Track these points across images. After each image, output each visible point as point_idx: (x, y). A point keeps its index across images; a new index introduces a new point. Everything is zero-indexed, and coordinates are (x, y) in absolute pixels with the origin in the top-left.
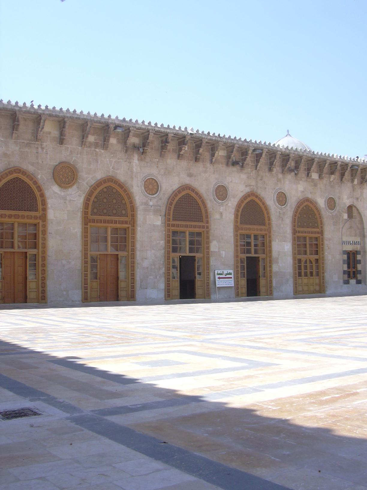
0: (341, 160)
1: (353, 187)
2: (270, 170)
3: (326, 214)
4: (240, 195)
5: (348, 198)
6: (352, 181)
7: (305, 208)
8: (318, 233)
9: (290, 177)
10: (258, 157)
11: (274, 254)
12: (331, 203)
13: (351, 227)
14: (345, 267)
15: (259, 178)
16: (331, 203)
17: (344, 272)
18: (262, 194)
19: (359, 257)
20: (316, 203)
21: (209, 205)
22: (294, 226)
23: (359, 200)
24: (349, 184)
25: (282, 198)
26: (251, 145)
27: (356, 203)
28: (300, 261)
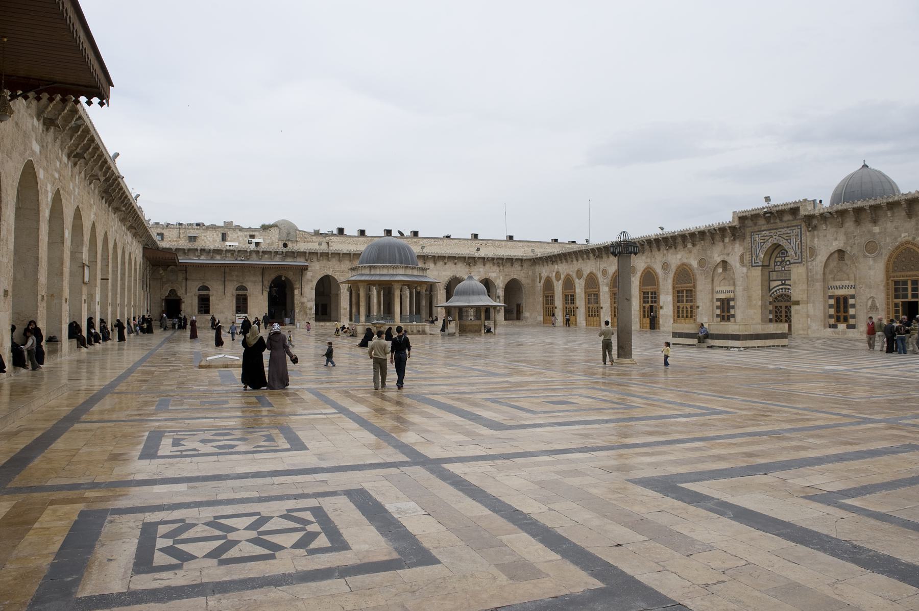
2: (659, 250)
4: (642, 269)
10: (642, 245)
11: (661, 304)
12: (702, 263)
14: (718, 312)
17: (718, 316)
19: (732, 303)
24: (721, 244)
27: (726, 259)
28: (678, 307)
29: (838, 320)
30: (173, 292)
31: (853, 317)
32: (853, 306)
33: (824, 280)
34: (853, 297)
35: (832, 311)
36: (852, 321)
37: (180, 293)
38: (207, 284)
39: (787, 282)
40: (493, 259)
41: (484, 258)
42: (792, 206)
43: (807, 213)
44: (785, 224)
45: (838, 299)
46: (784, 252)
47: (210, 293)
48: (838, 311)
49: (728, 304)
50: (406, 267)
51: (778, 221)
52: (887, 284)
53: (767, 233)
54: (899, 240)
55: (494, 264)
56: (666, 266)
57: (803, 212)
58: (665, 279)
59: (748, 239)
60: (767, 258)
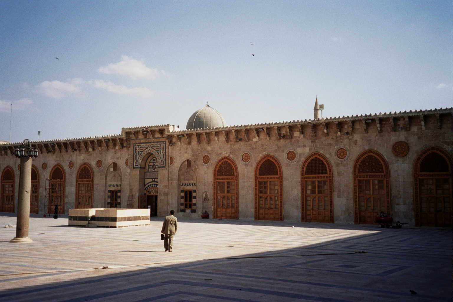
0: (96, 139)
1: (115, 151)
2: (67, 151)
3: (96, 170)
5: (111, 158)
6: (115, 148)
7: (87, 168)
8: (90, 181)
9: (77, 152)
10: (53, 146)
11: (67, 193)
12: (99, 163)
13: (114, 176)
15: (61, 156)
16: (99, 163)
18: (63, 164)
19: (119, 194)
20: (90, 165)
21: (40, 171)
22: (77, 178)
23: (119, 159)
24: (113, 151)
25: (71, 165)
26: (48, 143)
29: (186, 207)
31: (195, 204)
32: (195, 197)
33: (179, 179)
34: (195, 191)
35: (182, 201)
36: (194, 207)
39: (156, 180)
42: (160, 128)
43: (169, 134)
44: (155, 140)
45: (186, 192)
46: (154, 159)
48: (186, 201)
49: (116, 194)
51: (151, 137)
52: (214, 183)
53: (144, 145)
54: (221, 156)
56: (71, 165)
57: (166, 133)
58: (71, 175)
59: (132, 147)
60: (143, 163)
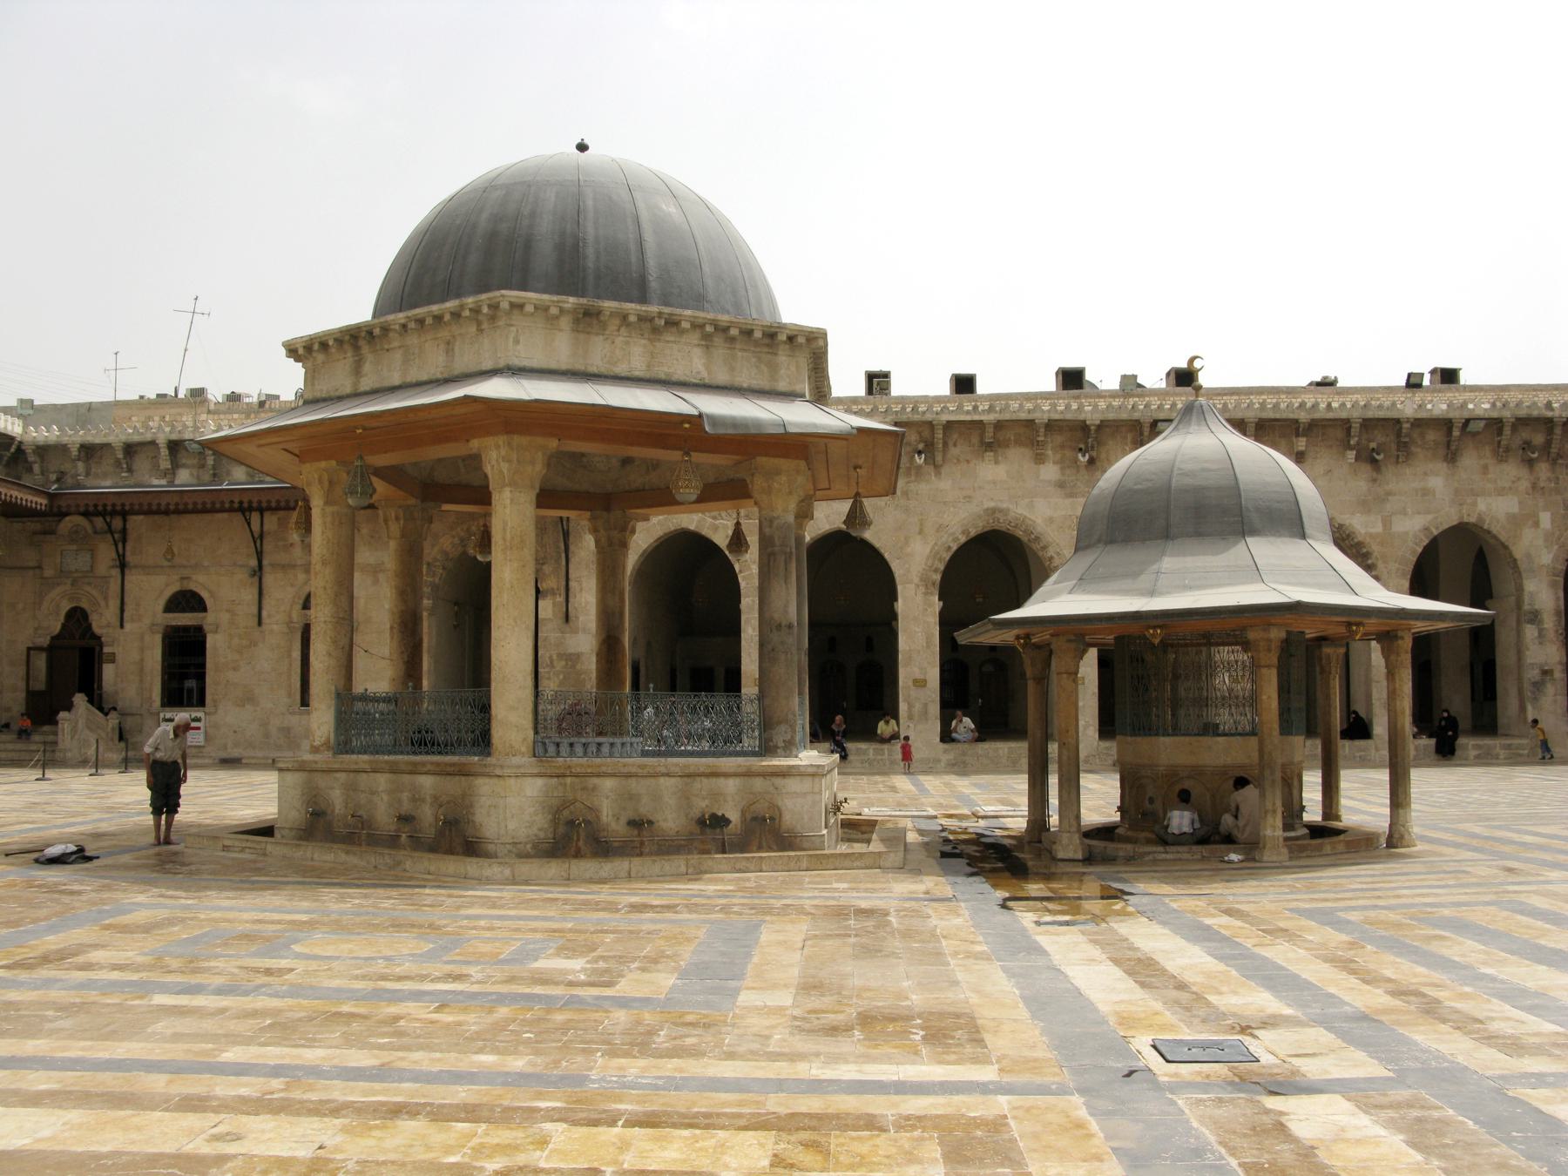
30: (77, 618)
37: (102, 621)
38: (200, 583)
40: (1495, 425)
41: (1445, 424)
47: (208, 620)
50: (588, 319)
55: (1502, 454)
